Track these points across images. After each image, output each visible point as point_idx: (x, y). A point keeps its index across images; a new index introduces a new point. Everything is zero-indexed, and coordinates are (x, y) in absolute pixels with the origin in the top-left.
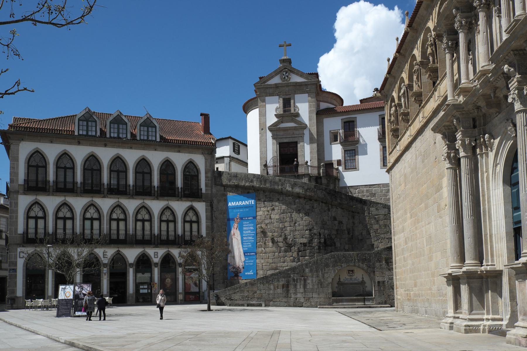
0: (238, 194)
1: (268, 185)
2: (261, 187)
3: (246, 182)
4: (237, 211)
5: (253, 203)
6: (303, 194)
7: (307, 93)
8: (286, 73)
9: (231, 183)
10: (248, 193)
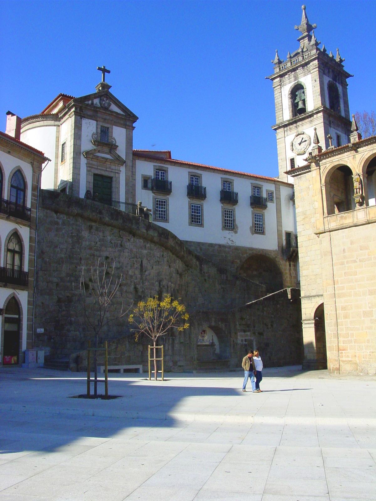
7: (125, 128)
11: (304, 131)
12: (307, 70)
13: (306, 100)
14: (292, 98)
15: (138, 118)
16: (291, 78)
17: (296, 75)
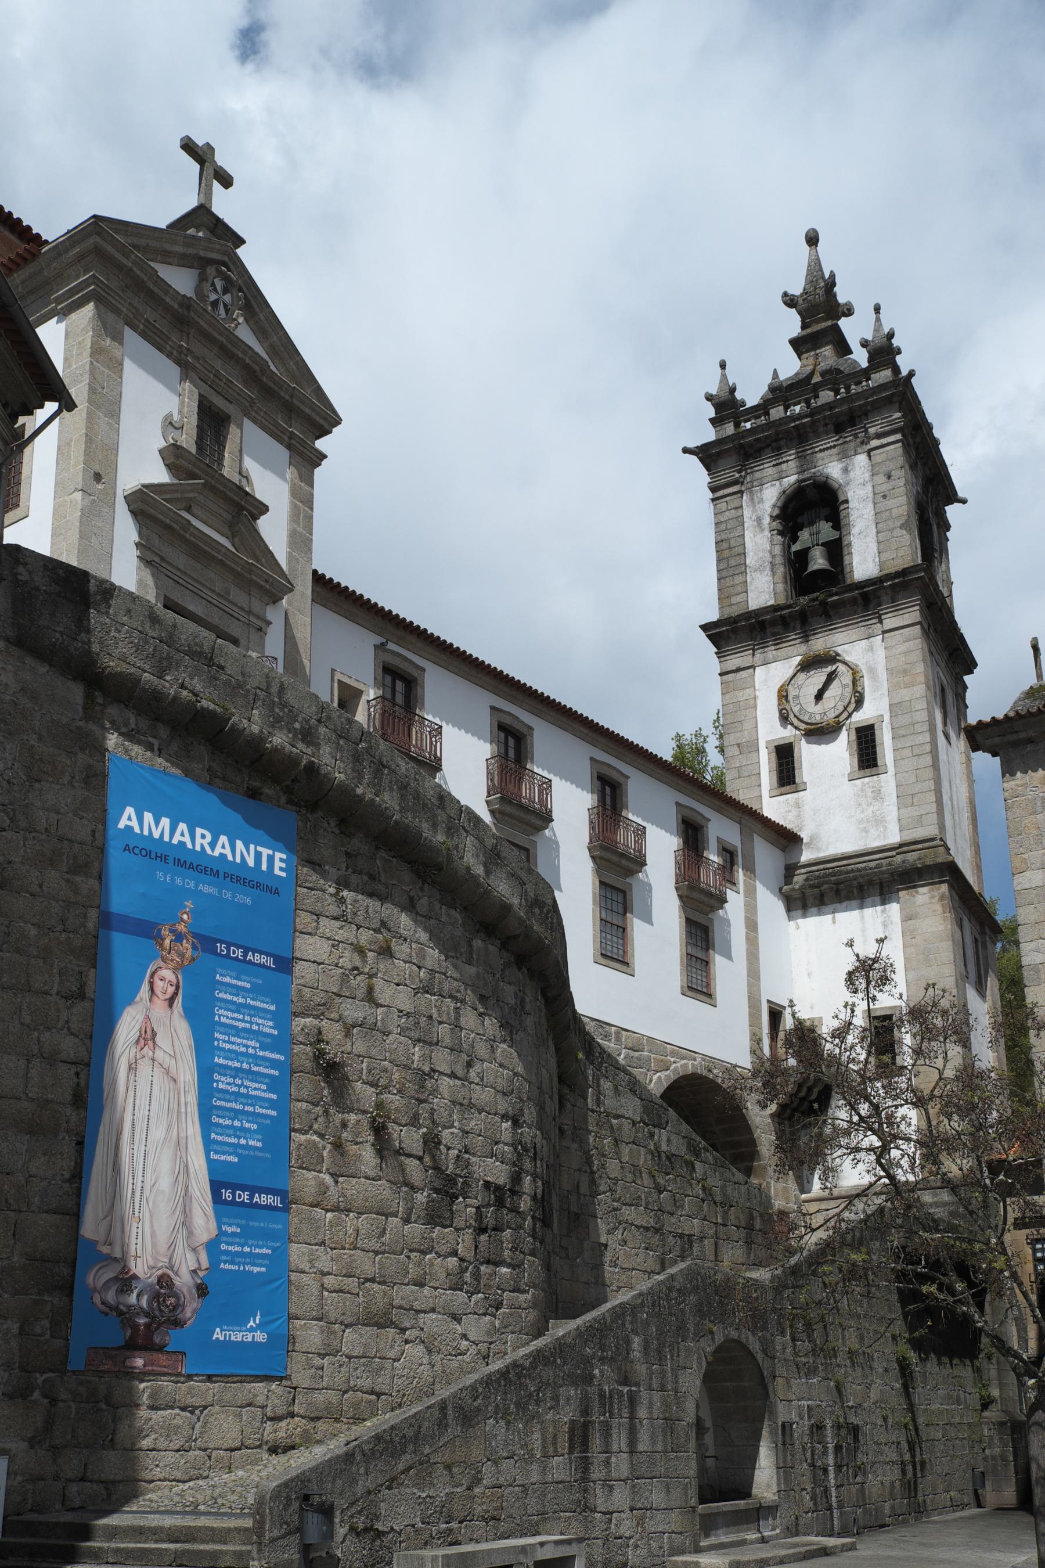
0: (187, 773)
1: (389, 800)
2: (359, 791)
3: (276, 722)
4: (178, 881)
5: (277, 872)
6: (520, 918)
7: (289, 447)
8: (226, 291)
9: (169, 686)
10: (253, 794)
11: (839, 650)
13: (845, 543)
15: (337, 421)
16: (784, 459)
17: (809, 452)
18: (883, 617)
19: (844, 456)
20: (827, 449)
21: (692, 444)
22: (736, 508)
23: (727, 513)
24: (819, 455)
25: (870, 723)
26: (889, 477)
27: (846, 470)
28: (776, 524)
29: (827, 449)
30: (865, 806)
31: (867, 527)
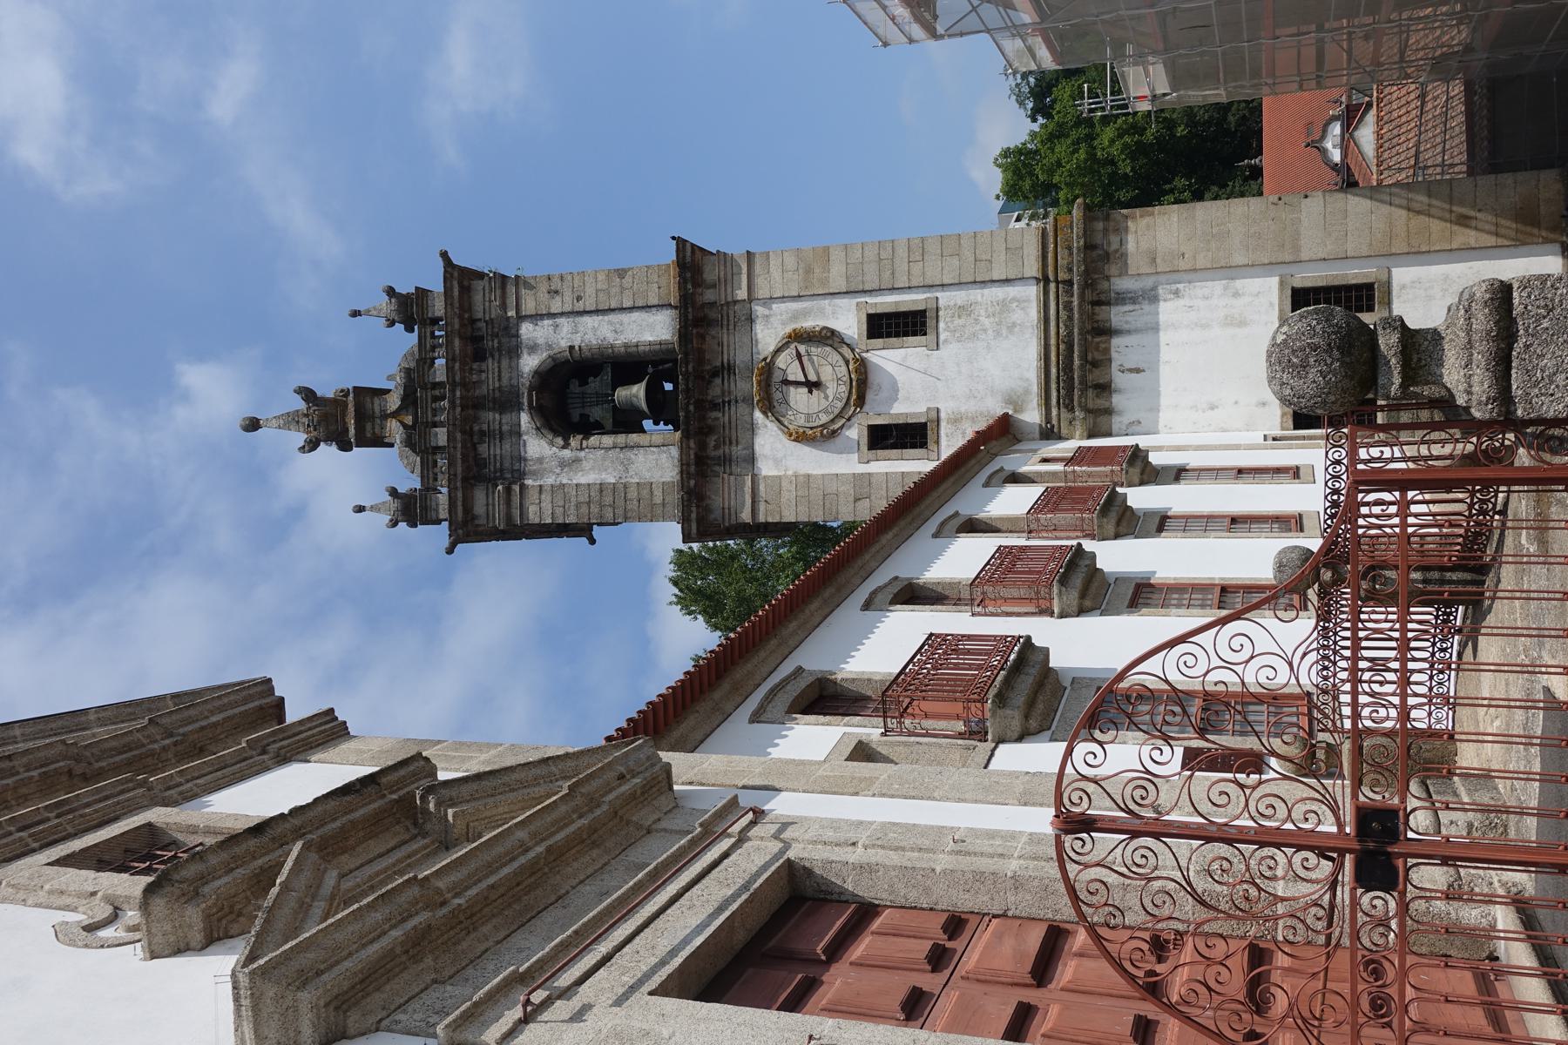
12: (496, 341)
14: (587, 434)
16: (497, 427)
18: (730, 299)
19: (514, 352)
20: (499, 371)
21: (446, 542)
22: (540, 492)
23: (543, 505)
24: (505, 381)
25: (864, 319)
26: (556, 292)
27: (533, 348)
28: (574, 442)
29: (499, 371)
30: (978, 327)
31: (610, 323)
